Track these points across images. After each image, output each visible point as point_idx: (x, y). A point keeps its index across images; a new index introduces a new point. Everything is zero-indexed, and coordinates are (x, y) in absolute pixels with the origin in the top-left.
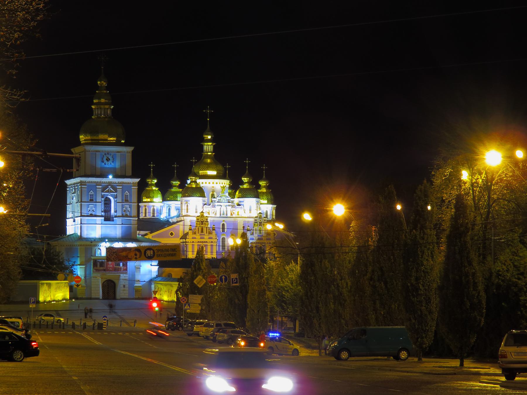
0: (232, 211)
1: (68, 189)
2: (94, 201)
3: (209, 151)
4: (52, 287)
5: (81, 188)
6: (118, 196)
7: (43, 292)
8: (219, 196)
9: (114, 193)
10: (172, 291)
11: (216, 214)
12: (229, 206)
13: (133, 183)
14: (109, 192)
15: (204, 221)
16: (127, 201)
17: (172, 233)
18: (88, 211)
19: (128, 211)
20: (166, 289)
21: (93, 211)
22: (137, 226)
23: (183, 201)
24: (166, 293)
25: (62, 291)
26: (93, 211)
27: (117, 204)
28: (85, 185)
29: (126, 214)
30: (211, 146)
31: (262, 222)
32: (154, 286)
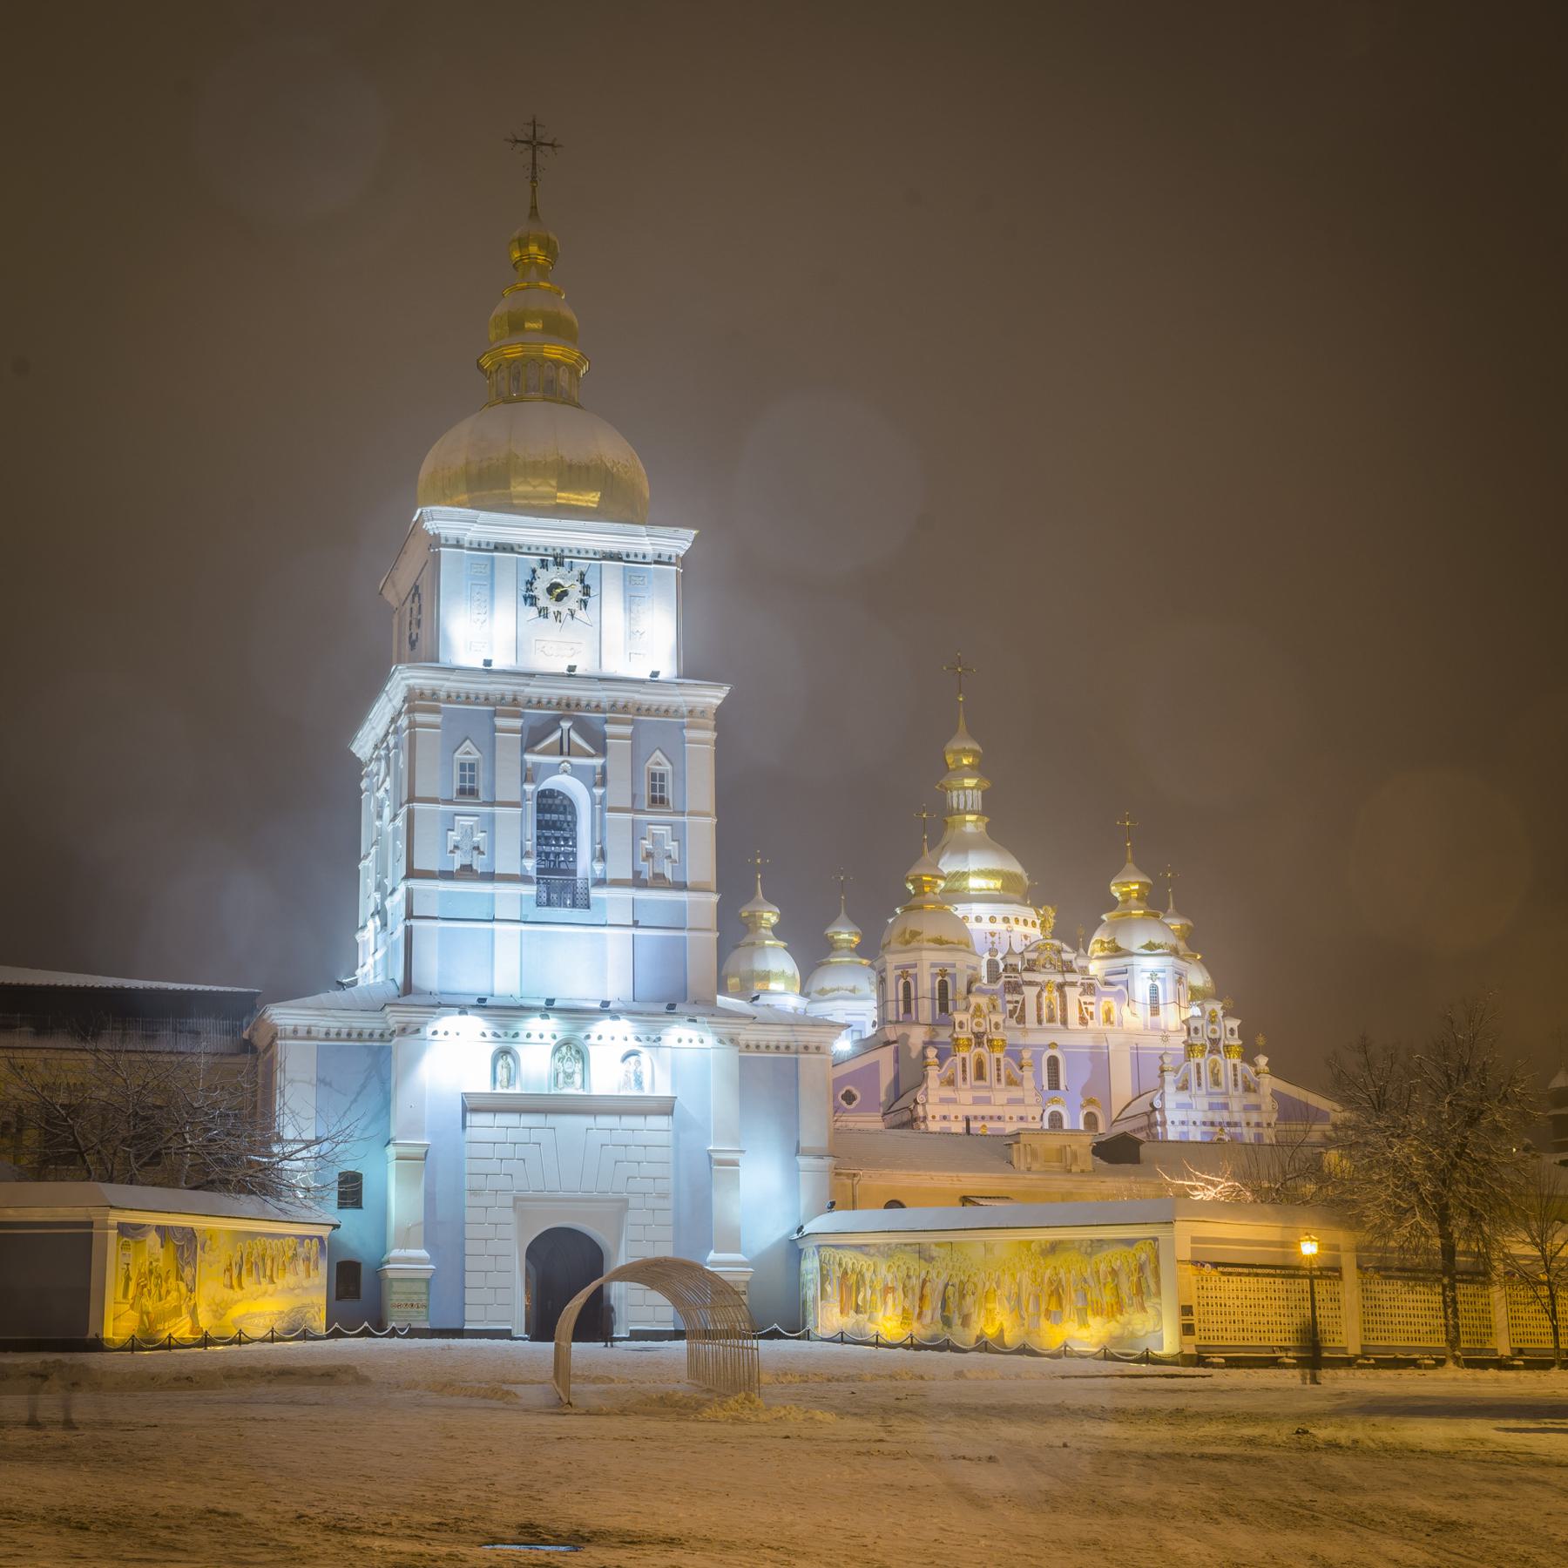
0: (1083, 1006)
1: (363, 785)
2: (483, 796)
3: (969, 807)
5: (412, 725)
6: (609, 776)
7: (132, 1285)
8: (1031, 949)
9: (590, 756)
10: (928, 1284)
11: (1021, 1019)
12: (1073, 984)
13: (691, 712)
14: (561, 753)
15: (984, 1033)
16: (658, 801)
17: (848, 1092)
18: (450, 847)
19: (670, 857)
20: (890, 1277)
21: (477, 848)
22: (715, 898)
23: (890, 967)
24: (890, 1297)
25: (281, 1282)
26: (477, 848)
27: (608, 815)
28: (436, 711)
29: (657, 870)
30: (975, 791)
31: (1220, 1039)
32: (816, 1264)
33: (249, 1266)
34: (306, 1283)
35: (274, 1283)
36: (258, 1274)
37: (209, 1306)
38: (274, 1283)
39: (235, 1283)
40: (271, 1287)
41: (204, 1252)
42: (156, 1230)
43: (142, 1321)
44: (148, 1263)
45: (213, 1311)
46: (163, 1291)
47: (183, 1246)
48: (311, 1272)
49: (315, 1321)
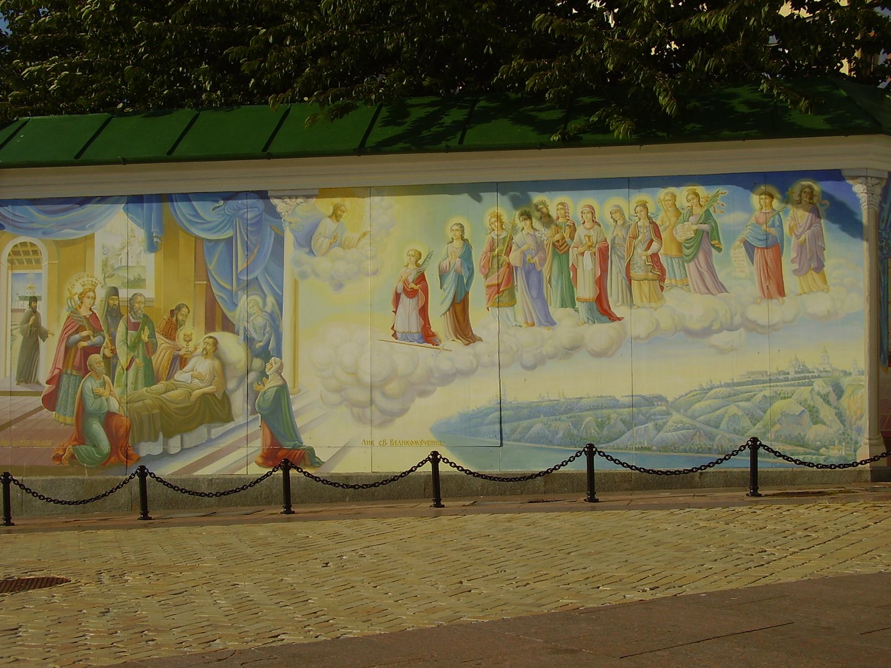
4: (322, 263)
33: (493, 280)
34: (761, 312)
35: (612, 318)
36: (541, 300)
37: (338, 390)
38: (612, 318)
39: (439, 323)
40: (602, 332)
41: (311, 252)
42: (127, 210)
43: (82, 436)
44: (101, 293)
45: (354, 404)
46: (161, 358)
47: (229, 241)
48: (790, 281)
49: (816, 420)
